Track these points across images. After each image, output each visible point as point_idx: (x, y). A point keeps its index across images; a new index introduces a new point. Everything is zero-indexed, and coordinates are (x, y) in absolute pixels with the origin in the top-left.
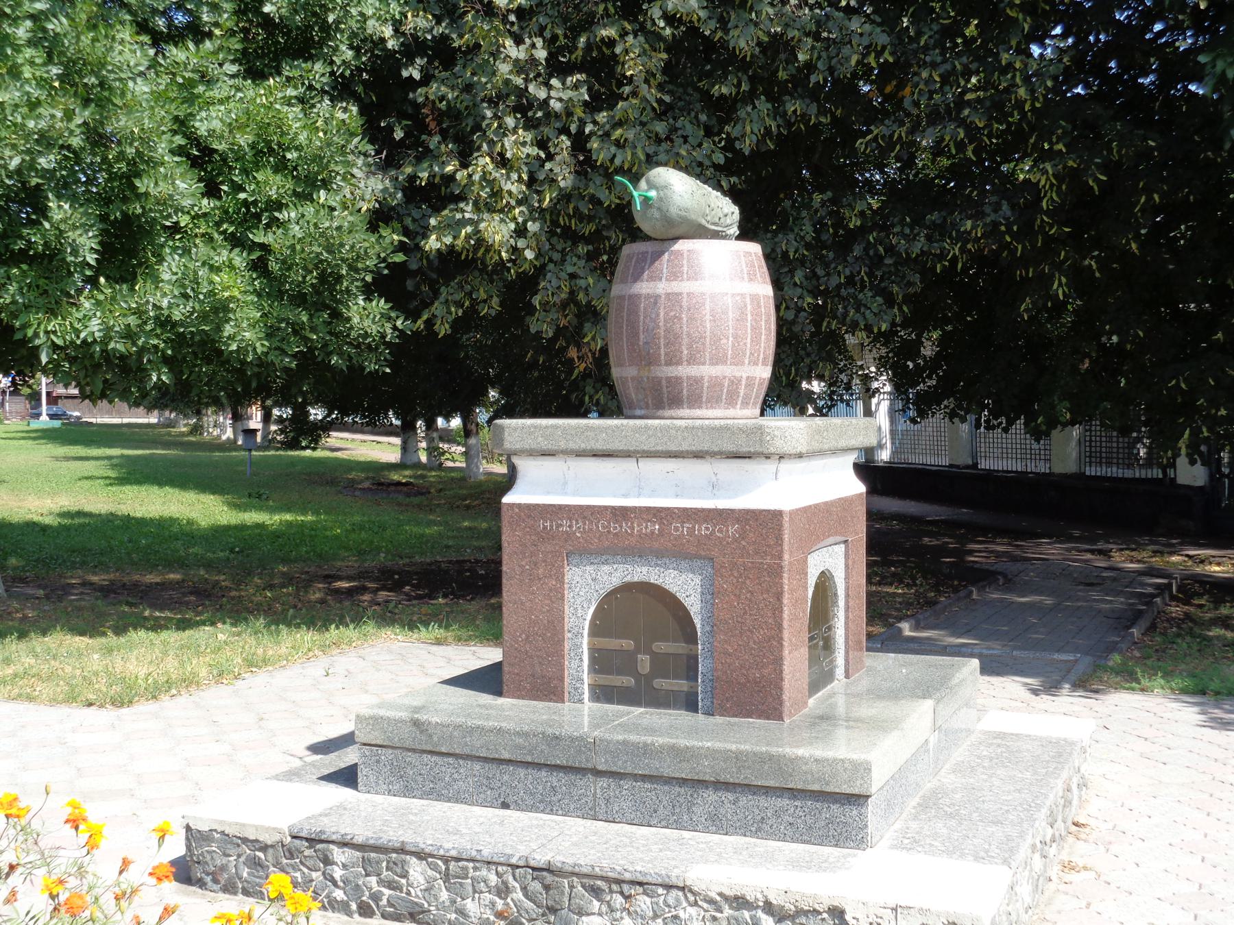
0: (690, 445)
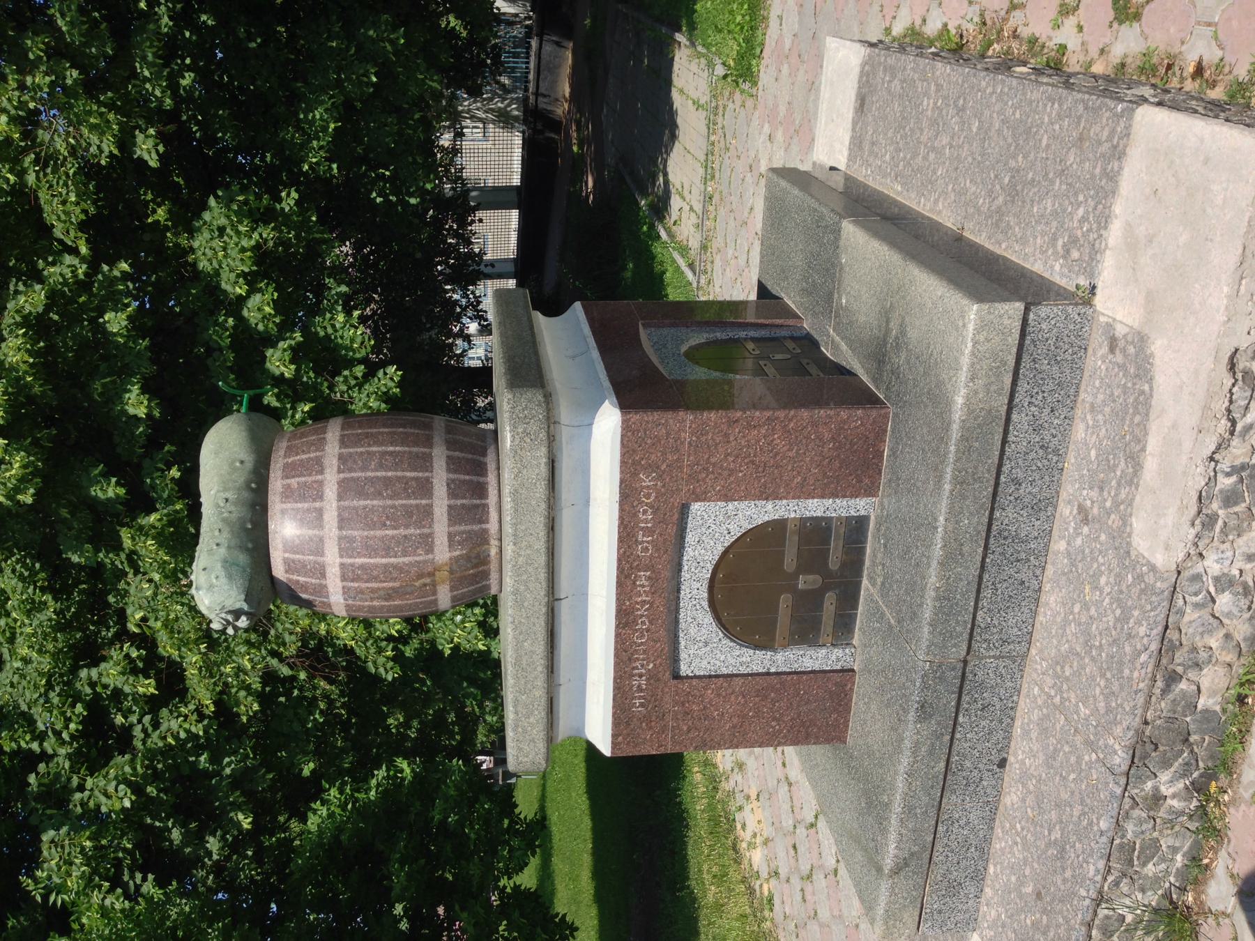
0: (538, 539)
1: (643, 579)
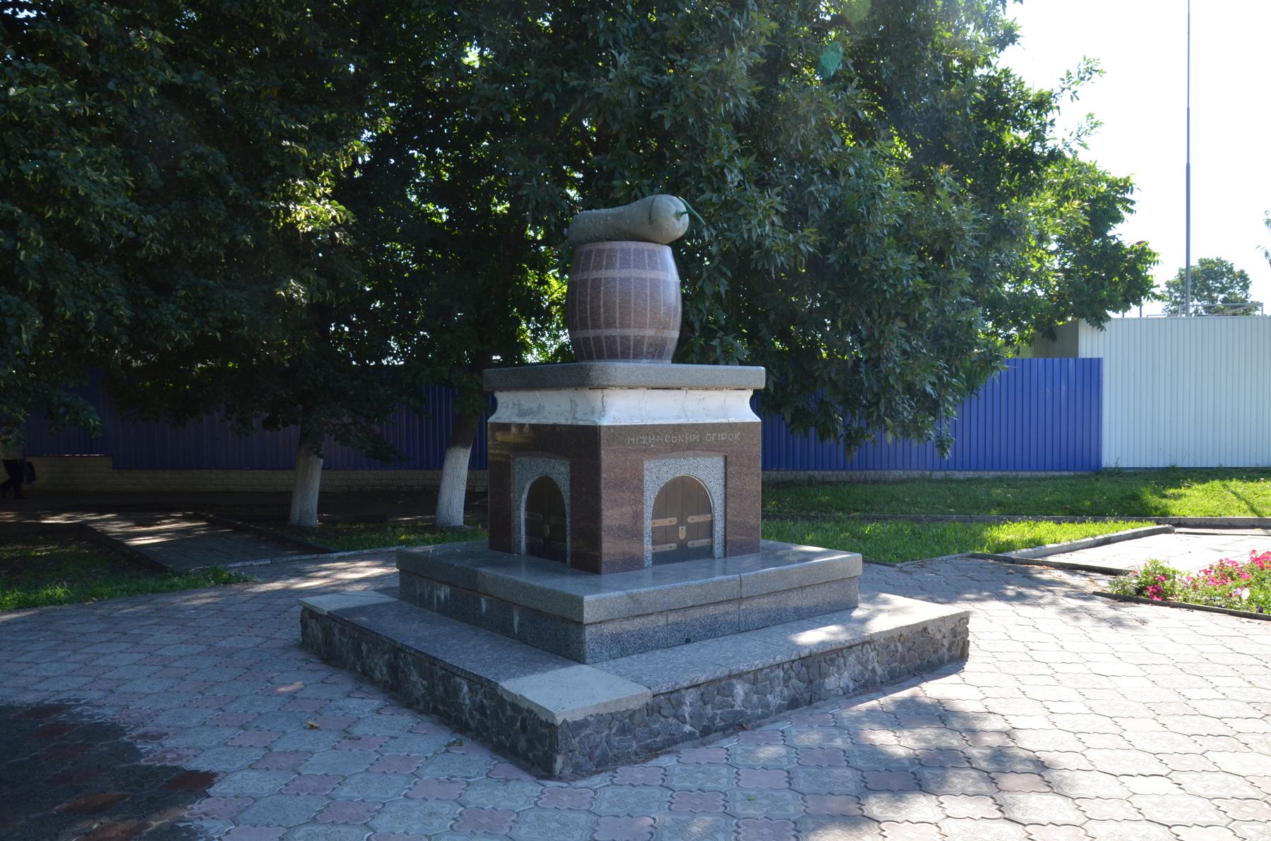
1: (696, 438)
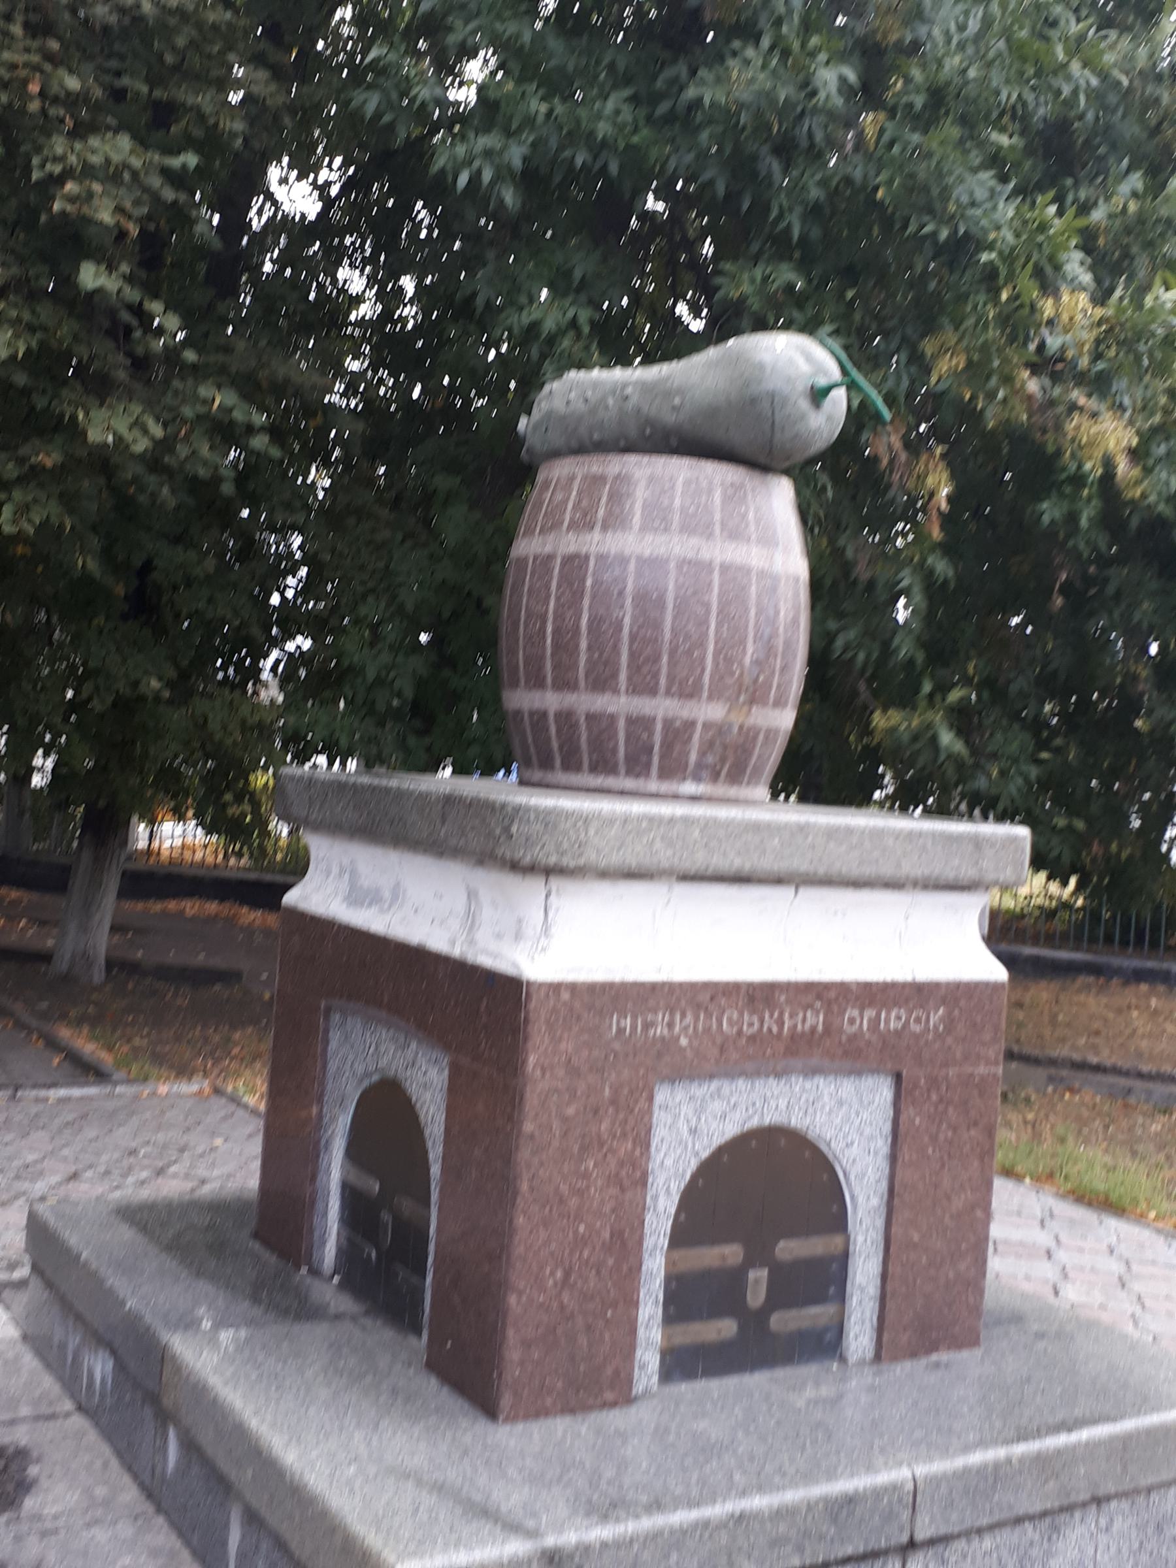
1: (815, 1020)
